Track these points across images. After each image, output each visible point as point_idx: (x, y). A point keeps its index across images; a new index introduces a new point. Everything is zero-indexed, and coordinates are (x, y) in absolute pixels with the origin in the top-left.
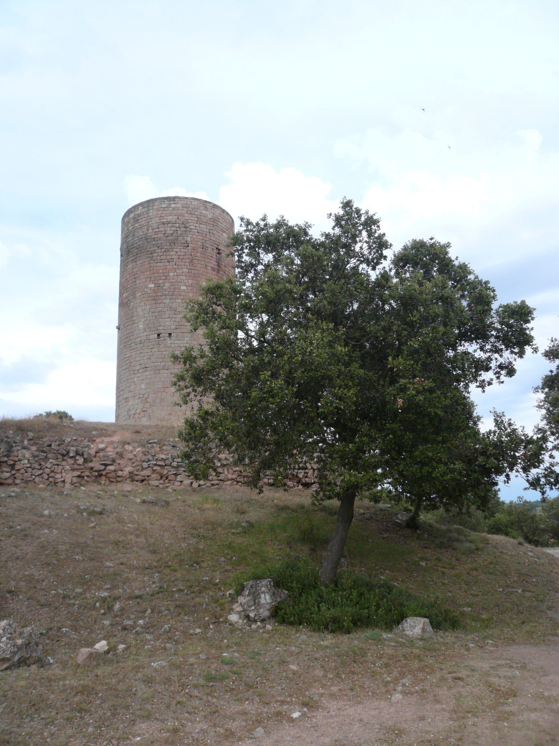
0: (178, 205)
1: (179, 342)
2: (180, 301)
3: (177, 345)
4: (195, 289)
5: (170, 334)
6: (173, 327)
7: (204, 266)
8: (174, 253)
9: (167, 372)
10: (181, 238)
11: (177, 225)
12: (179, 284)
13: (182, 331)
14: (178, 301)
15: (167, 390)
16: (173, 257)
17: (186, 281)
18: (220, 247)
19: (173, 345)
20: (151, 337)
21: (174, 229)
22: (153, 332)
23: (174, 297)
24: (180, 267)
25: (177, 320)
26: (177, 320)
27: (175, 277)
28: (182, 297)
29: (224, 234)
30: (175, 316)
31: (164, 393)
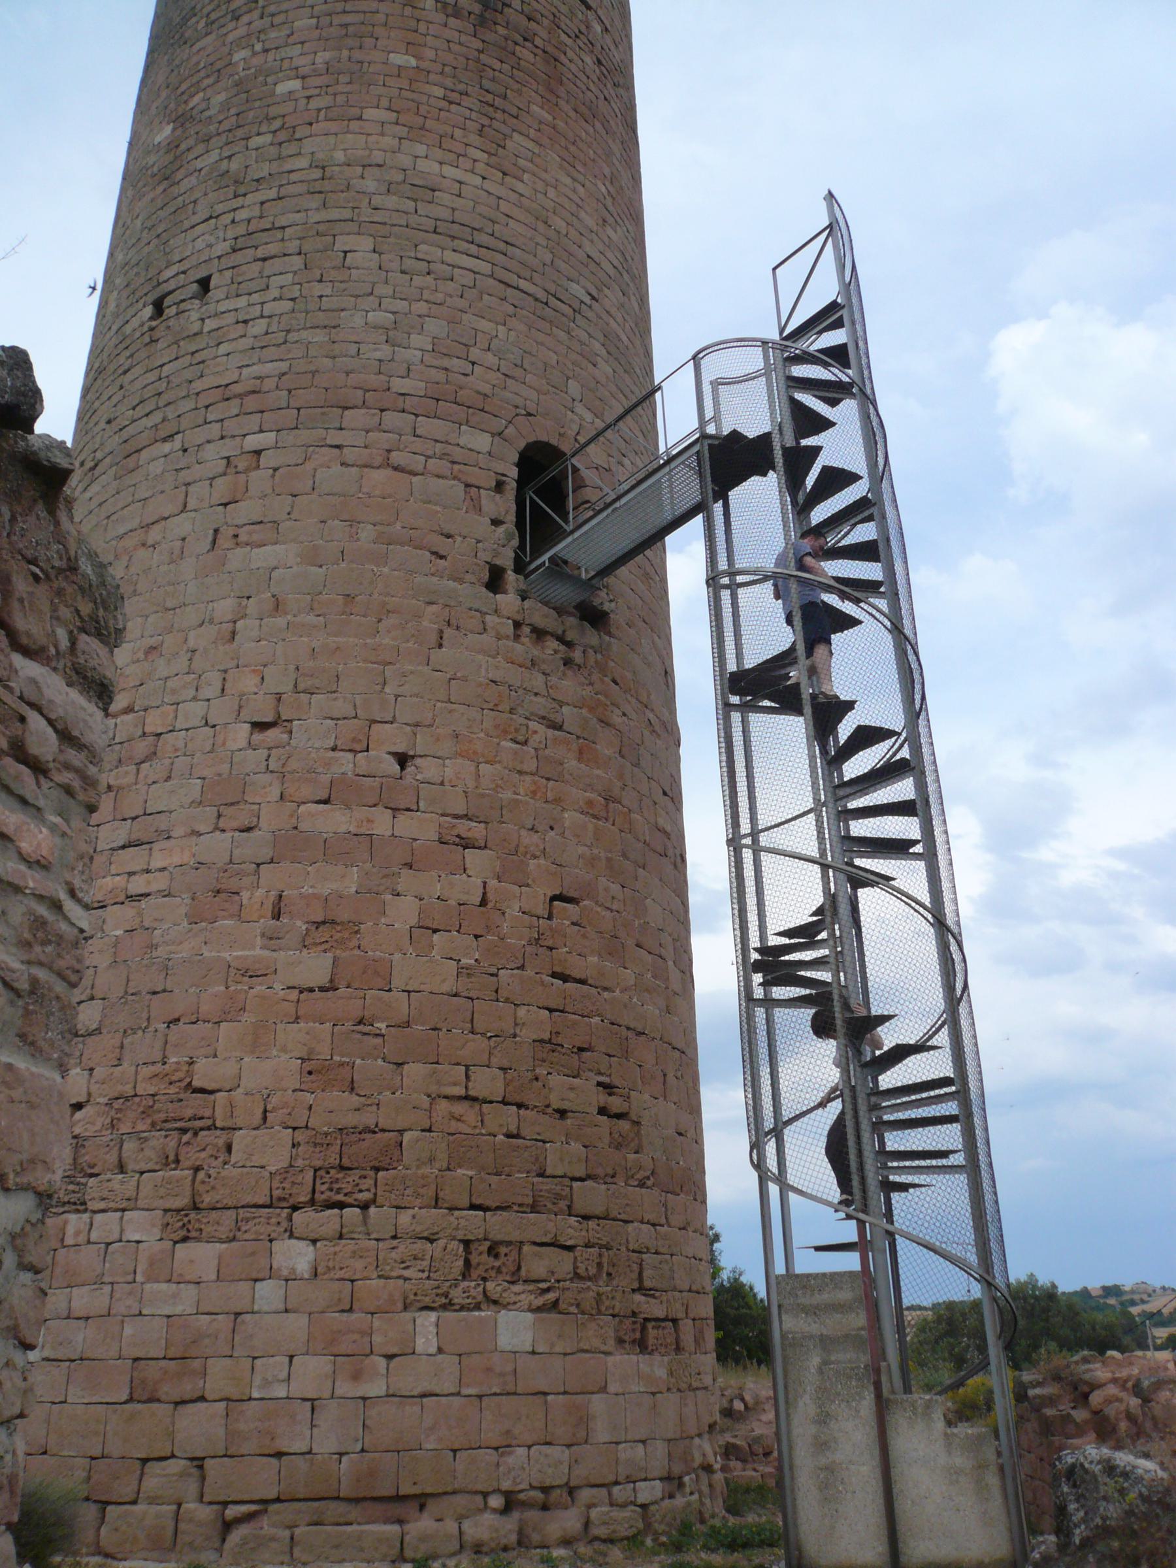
1: (242, 302)
2: (268, 138)
3: (230, 318)
4: (343, 79)
5: (204, 284)
6: (222, 247)
9: (167, 447)
12: (269, 80)
13: (260, 253)
14: (256, 141)
15: (154, 534)
17: (298, 62)
19: (210, 324)
20: (135, 322)
22: (140, 304)
23: (240, 133)
24: (277, 20)
25: (242, 215)
26: (242, 215)
27: (255, 61)
28: (277, 124)
31: (142, 553)
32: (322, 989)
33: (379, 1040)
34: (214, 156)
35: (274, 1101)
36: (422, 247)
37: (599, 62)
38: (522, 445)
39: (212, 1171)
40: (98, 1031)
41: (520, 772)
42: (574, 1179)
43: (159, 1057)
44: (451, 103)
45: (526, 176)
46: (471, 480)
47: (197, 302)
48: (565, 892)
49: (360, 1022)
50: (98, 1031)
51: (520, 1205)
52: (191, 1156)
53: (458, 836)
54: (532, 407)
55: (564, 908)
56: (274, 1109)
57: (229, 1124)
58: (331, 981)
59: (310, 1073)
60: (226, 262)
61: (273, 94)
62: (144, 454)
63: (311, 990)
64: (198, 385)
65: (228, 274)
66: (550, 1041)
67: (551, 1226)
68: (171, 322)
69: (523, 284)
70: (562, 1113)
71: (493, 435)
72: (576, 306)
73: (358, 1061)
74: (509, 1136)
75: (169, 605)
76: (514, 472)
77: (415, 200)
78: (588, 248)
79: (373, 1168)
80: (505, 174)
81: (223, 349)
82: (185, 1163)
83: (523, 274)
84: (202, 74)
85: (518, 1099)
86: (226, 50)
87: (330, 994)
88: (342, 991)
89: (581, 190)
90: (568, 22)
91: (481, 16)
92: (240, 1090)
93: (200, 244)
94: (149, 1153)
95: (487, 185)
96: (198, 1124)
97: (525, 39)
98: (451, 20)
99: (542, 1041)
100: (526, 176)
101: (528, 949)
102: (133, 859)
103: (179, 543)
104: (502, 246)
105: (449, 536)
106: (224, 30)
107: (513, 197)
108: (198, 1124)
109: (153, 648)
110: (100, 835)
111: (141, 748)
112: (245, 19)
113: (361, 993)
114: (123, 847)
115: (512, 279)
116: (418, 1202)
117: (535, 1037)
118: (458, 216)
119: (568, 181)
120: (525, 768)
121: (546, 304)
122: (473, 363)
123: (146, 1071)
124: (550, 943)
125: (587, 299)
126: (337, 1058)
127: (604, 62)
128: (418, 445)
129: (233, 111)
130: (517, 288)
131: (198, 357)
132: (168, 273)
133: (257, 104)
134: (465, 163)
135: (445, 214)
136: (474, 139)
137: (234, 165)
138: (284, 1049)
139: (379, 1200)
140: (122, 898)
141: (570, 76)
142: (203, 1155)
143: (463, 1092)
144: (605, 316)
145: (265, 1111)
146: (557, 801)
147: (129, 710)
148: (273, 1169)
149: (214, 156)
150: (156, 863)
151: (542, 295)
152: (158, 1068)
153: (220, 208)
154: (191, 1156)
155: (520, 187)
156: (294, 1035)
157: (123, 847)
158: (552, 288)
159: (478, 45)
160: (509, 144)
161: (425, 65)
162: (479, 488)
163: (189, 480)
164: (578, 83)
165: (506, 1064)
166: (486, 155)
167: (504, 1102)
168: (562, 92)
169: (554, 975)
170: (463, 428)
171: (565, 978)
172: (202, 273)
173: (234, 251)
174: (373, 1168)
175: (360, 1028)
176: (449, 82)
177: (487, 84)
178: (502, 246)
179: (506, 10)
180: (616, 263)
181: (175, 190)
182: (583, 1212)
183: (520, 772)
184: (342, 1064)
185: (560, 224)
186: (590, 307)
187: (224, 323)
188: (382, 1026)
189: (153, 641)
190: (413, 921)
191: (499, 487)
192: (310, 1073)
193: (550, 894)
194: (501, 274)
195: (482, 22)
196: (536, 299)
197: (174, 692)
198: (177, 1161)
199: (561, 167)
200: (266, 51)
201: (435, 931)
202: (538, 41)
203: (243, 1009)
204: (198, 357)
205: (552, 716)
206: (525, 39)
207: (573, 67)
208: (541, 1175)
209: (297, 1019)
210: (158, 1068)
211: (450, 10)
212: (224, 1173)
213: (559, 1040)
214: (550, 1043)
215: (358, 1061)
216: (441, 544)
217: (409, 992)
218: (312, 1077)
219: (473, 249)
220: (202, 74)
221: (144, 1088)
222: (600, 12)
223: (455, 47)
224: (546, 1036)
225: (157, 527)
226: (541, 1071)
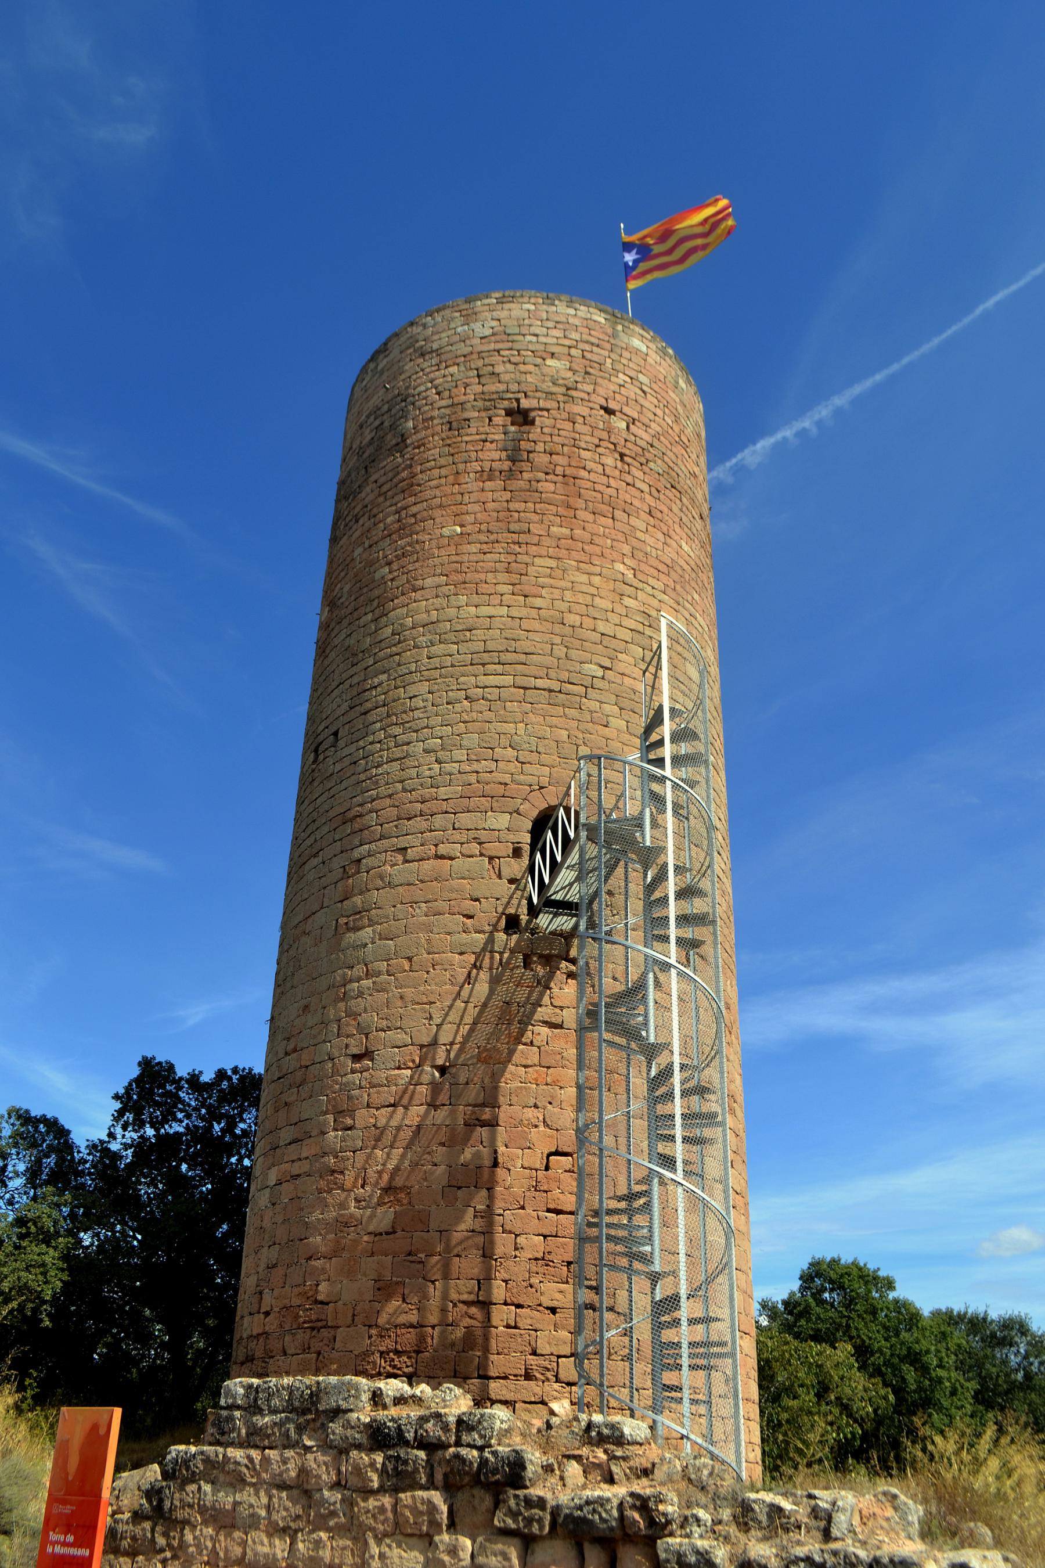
0: (391, 356)
2: (370, 616)
3: (347, 761)
6: (345, 706)
7: (451, 478)
8: (368, 489)
10: (389, 437)
11: (386, 407)
12: (372, 570)
16: (367, 501)
18: (525, 404)
19: (338, 767)
21: (377, 423)
25: (355, 680)
26: (355, 680)
28: (375, 603)
29: (550, 362)
30: (355, 669)
32: (387, 1233)
33: (421, 1266)
34: (343, 635)
35: (358, 1308)
36: (462, 679)
37: (622, 455)
38: (535, 813)
39: (325, 1354)
40: (275, 1266)
41: (525, 1067)
42: (559, 1357)
43: (301, 1281)
44: (485, 553)
45: (544, 592)
46: (493, 853)
47: (333, 749)
48: (560, 1150)
49: (410, 1254)
50: (275, 1266)
51: (515, 1376)
52: (316, 1345)
53: (477, 1119)
54: (544, 781)
55: (558, 1161)
56: (359, 1313)
57: (334, 1324)
58: (393, 1227)
59: (379, 1289)
60: (347, 718)
61: (374, 581)
62: (307, 867)
63: (381, 1234)
64: (332, 814)
65: (347, 727)
66: (543, 1259)
67: (538, 1390)
68: (321, 766)
69: (539, 683)
70: (553, 1310)
71: (511, 813)
72: (588, 683)
73: (407, 1280)
74: (508, 1326)
75: (314, 976)
76: (527, 838)
77: (456, 643)
78: (602, 627)
79: (414, 1351)
80: (526, 596)
81: (344, 784)
82: (312, 1350)
83: (537, 674)
84: (340, 568)
85: (516, 1301)
86: (351, 548)
87: (392, 1236)
88: (400, 1233)
89: (596, 580)
90: (588, 438)
91: (511, 470)
92: (341, 1302)
93: (335, 705)
94: (296, 1343)
95: (514, 612)
96: (320, 1324)
97: (547, 474)
98: (488, 483)
99: (536, 1259)
100: (544, 592)
101: (528, 1194)
102: (292, 1152)
103: (319, 931)
104: (522, 658)
105: (477, 900)
106: (351, 532)
107: (534, 613)
108: (320, 1324)
109: (306, 1007)
110: (281, 1135)
111: (299, 1075)
112: (361, 522)
113: (410, 1235)
114: (290, 1144)
115: (532, 682)
116: (442, 1374)
117: (531, 1257)
118: (490, 645)
119: (584, 578)
120: (529, 1063)
121: (560, 691)
122: (496, 761)
123: (296, 1290)
124: (545, 1188)
125: (600, 673)
126: (394, 1279)
127: (627, 452)
128: (457, 836)
129: (353, 598)
130: (535, 688)
131: (332, 792)
132: (321, 728)
133: (365, 590)
134: (495, 600)
135: (480, 646)
136: (503, 577)
137: (352, 641)
138: (365, 1275)
139: (419, 1372)
140: (288, 1178)
141: (589, 485)
142: (321, 1344)
143: (472, 1297)
144: (618, 679)
145: (354, 1315)
146: (555, 1083)
147: (295, 1050)
148: (356, 1353)
149: (343, 635)
150: (304, 1155)
151: (555, 685)
152: (301, 1289)
153: (345, 676)
154: (316, 1345)
155: (538, 602)
156: (370, 1264)
157: (290, 1144)
158: (565, 675)
159: (508, 495)
160: (531, 570)
161: (469, 529)
162: (499, 858)
163: (325, 885)
164: (598, 487)
165: (507, 1277)
166: (511, 587)
167: (506, 1304)
168: (580, 503)
169: (549, 1210)
170: (490, 813)
171: (558, 1212)
172: (333, 729)
173: (351, 708)
174: (414, 1351)
175: (410, 1258)
176: (483, 538)
177: (514, 527)
178: (522, 658)
179: (531, 455)
180: (633, 625)
181: (326, 662)
182: (566, 1380)
183: (525, 1067)
184: (397, 1283)
185: (573, 619)
186: (603, 678)
187: (345, 765)
188: (422, 1256)
189: (304, 1002)
190: (445, 1182)
191: (517, 853)
192: (379, 1289)
193: (546, 1152)
194: (522, 681)
195: (510, 475)
196: (551, 691)
197: (315, 1037)
198: (309, 1348)
199: (578, 569)
200: (370, 546)
201: (459, 1188)
202: (559, 470)
203: (343, 1249)
204: (332, 792)
205: (553, 1020)
206: (547, 474)
207: (593, 477)
208: (534, 1353)
209: (372, 1254)
210: (301, 1289)
211: (485, 477)
212: (332, 1356)
213: (550, 1257)
214: (544, 1260)
215: (407, 1280)
216: (469, 906)
217: (441, 1232)
218: (380, 1292)
219: (499, 668)
220: (340, 568)
221: (296, 1302)
222: (626, 409)
223: (490, 506)
224: (540, 1255)
225: (310, 920)
226: (535, 1281)
